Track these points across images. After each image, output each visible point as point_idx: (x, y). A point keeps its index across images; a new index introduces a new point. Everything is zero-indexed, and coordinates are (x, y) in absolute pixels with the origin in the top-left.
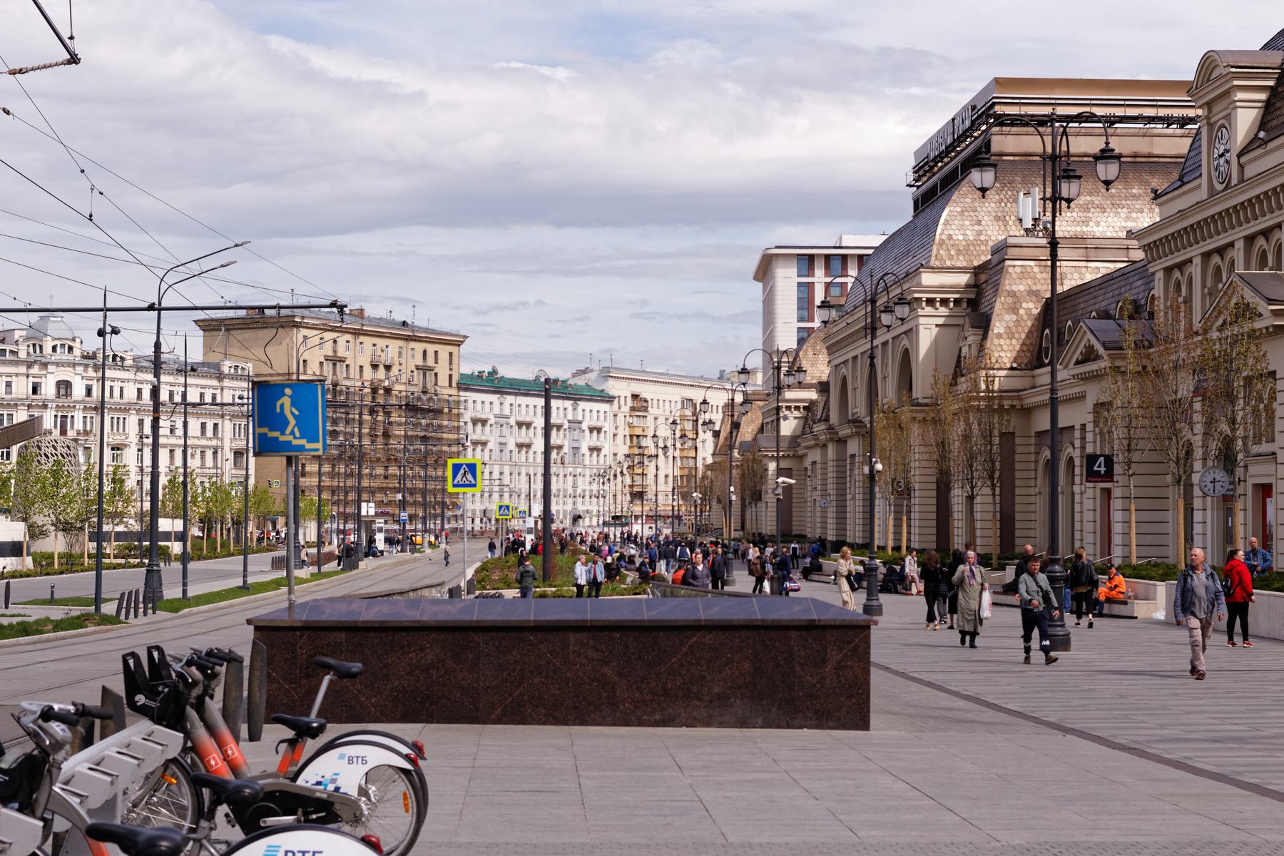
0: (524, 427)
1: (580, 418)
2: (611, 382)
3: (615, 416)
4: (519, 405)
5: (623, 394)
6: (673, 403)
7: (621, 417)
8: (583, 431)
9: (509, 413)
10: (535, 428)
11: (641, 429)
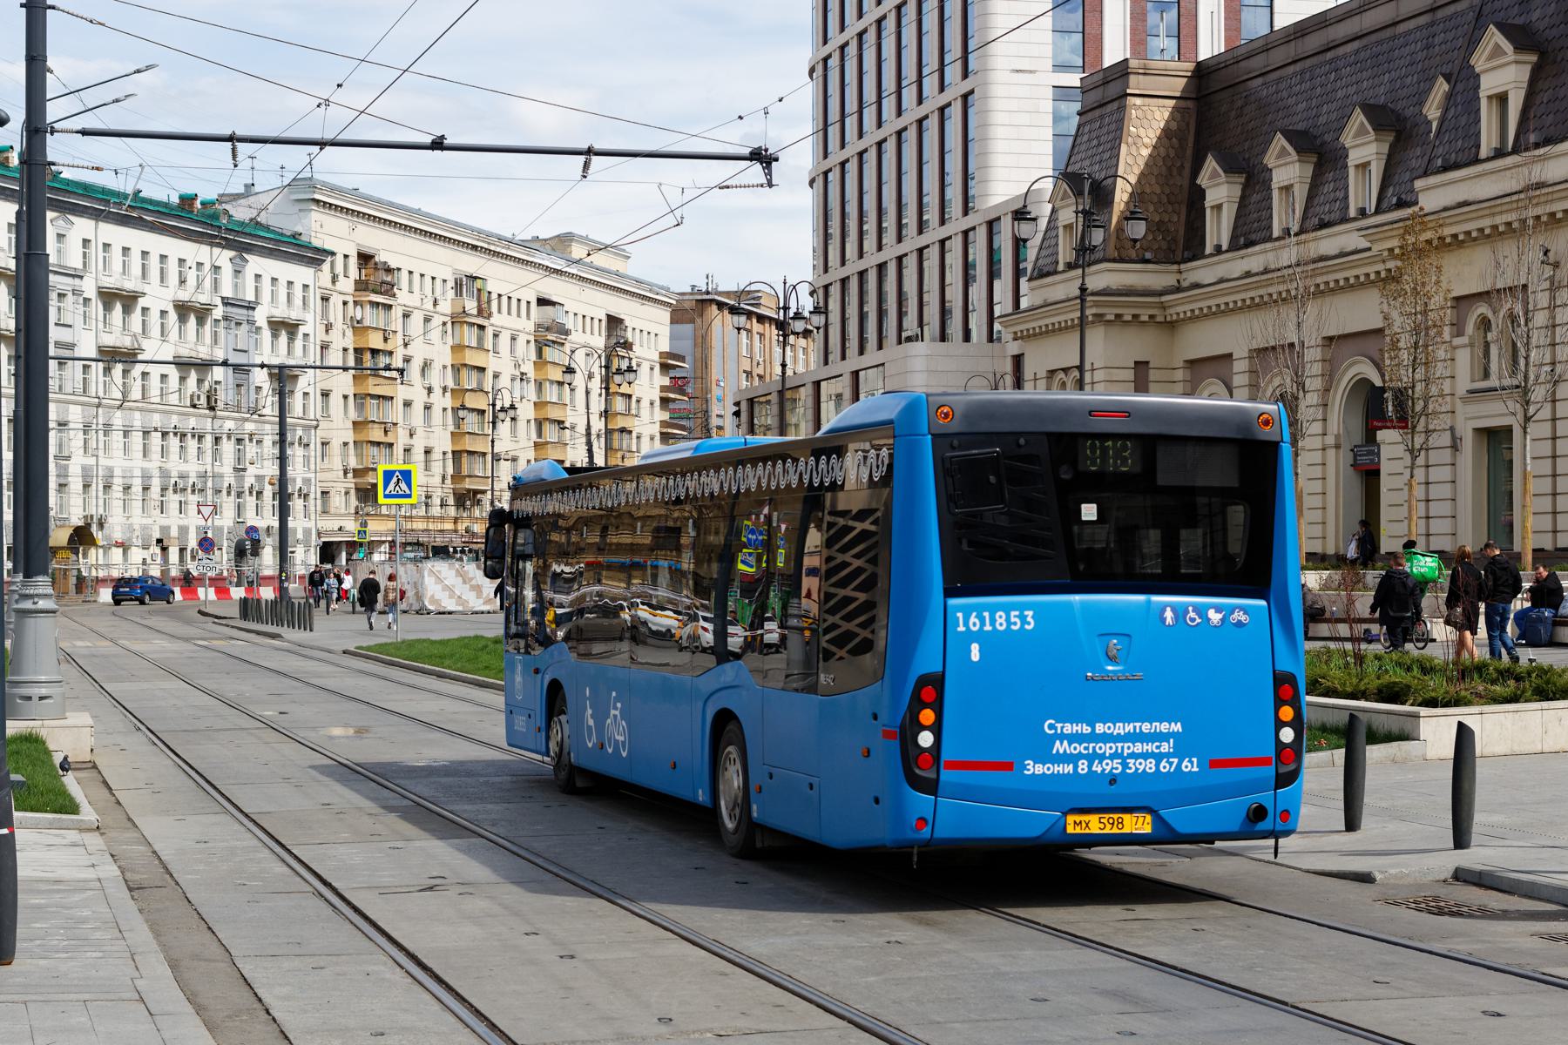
0: (118, 307)
1: (250, 297)
2: (317, 216)
3: (325, 299)
4: (106, 246)
5: (340, 247)
6: (438, 282)
7: (336, 301)
8: (259, 329)
9: (81, 267)
10: (145, 310)
11: (380, 335)
